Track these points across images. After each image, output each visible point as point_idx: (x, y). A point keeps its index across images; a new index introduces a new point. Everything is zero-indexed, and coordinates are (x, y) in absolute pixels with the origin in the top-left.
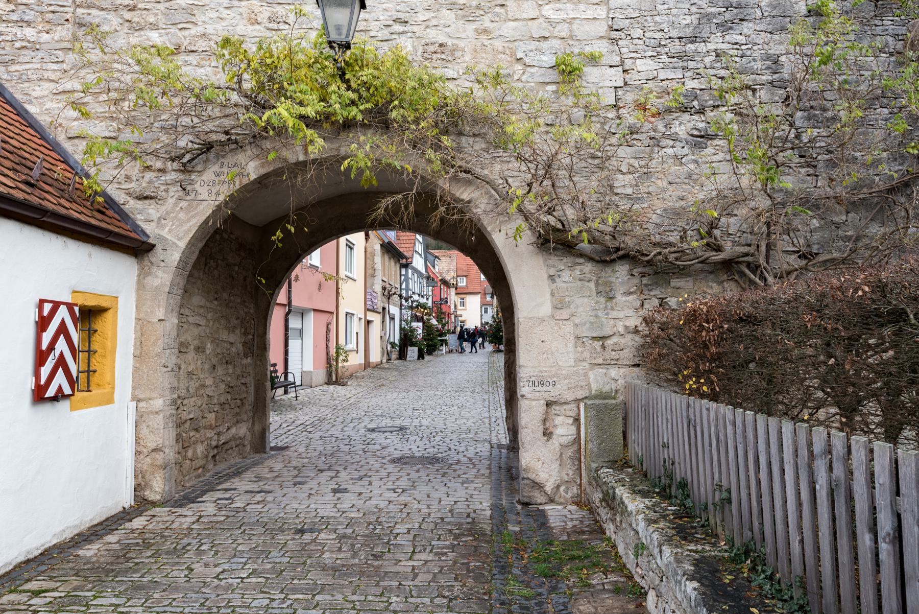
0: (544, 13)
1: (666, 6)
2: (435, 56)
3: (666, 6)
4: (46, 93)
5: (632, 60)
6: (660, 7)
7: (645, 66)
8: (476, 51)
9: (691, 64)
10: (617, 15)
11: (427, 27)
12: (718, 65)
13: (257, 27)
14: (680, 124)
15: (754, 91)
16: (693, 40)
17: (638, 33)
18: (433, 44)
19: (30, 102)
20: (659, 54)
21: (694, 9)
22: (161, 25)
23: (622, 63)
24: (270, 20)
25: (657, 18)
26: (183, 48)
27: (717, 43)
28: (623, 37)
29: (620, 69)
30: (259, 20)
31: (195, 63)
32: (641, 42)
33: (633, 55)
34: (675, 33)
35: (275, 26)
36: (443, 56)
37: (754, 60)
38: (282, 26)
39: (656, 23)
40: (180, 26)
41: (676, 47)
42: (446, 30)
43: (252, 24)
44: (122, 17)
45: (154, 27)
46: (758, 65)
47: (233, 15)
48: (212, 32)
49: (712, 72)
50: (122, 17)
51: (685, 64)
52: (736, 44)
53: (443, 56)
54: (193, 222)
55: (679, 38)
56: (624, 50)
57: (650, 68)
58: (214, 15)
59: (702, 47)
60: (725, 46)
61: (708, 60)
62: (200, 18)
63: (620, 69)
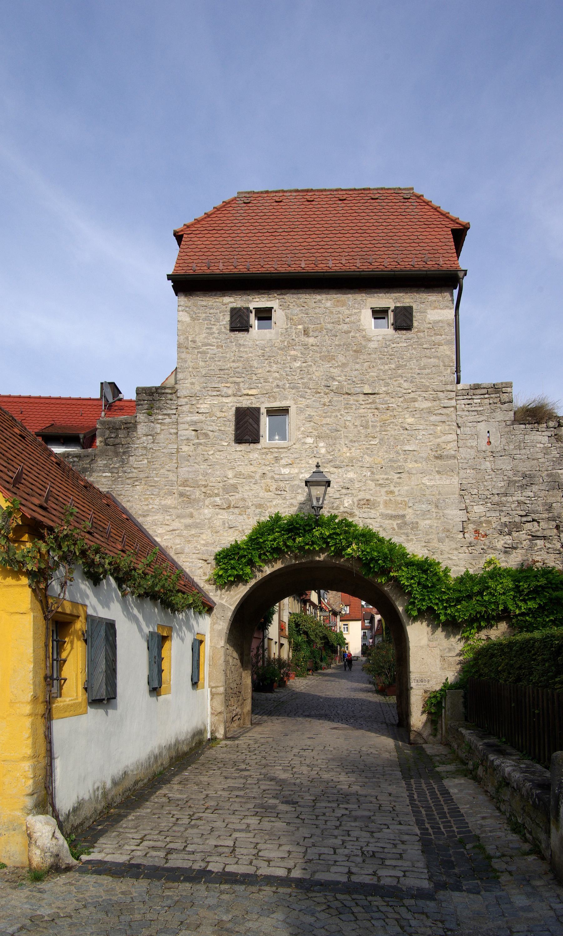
0: (423, 482)
1: (490, 477)
3: (490, 477)
4: (164, 531)
5: (471, 507)
7: (478, 509)
8: (386, 503)
9: (504, 508)
10: (464, 482)
11: (360, 491)
13: (270, 493)
14: (498, 541)
15: (538, 522)
16: (506, 495)
17: (475, 491)
19: (157, 536)
20: (486, 503)
21: (506, 478)
22: (220, 494)
23: (466, 508)
24: (277, 489)
25: (485, 483)
26: (232, 506)
27: (518, 496)
28: (467, 494)
29: (465, 511)
30: (271, 490)
31: (238, 513)
32: (477, 496)
33: (472, 504)
34: (495, 492)
35: (280, 493)
36: (369, 506)
37: (538, 506)
38: (283, 493)
39: (485, 486)
40: (231, 494)
41: (496, 499)
42: (371, 492)
43: (267, 492)
44: (201, 490)
45: (217, 495)
46: (540, 508)
47: (257, 487)
48: (247, 497)
49: (514, 512)
50: (201, 490)
51: (501, 508)
52: (529, 497)
53: (369, 506)
54: (239, 596)
55: (497, 494)
56: (467, 501)
57: (481, 511)
58: (247, 488)
59: (510, 499)
60: (523, 499)
61: (513, 506)
62: (240, 489)
63: (465, 511)
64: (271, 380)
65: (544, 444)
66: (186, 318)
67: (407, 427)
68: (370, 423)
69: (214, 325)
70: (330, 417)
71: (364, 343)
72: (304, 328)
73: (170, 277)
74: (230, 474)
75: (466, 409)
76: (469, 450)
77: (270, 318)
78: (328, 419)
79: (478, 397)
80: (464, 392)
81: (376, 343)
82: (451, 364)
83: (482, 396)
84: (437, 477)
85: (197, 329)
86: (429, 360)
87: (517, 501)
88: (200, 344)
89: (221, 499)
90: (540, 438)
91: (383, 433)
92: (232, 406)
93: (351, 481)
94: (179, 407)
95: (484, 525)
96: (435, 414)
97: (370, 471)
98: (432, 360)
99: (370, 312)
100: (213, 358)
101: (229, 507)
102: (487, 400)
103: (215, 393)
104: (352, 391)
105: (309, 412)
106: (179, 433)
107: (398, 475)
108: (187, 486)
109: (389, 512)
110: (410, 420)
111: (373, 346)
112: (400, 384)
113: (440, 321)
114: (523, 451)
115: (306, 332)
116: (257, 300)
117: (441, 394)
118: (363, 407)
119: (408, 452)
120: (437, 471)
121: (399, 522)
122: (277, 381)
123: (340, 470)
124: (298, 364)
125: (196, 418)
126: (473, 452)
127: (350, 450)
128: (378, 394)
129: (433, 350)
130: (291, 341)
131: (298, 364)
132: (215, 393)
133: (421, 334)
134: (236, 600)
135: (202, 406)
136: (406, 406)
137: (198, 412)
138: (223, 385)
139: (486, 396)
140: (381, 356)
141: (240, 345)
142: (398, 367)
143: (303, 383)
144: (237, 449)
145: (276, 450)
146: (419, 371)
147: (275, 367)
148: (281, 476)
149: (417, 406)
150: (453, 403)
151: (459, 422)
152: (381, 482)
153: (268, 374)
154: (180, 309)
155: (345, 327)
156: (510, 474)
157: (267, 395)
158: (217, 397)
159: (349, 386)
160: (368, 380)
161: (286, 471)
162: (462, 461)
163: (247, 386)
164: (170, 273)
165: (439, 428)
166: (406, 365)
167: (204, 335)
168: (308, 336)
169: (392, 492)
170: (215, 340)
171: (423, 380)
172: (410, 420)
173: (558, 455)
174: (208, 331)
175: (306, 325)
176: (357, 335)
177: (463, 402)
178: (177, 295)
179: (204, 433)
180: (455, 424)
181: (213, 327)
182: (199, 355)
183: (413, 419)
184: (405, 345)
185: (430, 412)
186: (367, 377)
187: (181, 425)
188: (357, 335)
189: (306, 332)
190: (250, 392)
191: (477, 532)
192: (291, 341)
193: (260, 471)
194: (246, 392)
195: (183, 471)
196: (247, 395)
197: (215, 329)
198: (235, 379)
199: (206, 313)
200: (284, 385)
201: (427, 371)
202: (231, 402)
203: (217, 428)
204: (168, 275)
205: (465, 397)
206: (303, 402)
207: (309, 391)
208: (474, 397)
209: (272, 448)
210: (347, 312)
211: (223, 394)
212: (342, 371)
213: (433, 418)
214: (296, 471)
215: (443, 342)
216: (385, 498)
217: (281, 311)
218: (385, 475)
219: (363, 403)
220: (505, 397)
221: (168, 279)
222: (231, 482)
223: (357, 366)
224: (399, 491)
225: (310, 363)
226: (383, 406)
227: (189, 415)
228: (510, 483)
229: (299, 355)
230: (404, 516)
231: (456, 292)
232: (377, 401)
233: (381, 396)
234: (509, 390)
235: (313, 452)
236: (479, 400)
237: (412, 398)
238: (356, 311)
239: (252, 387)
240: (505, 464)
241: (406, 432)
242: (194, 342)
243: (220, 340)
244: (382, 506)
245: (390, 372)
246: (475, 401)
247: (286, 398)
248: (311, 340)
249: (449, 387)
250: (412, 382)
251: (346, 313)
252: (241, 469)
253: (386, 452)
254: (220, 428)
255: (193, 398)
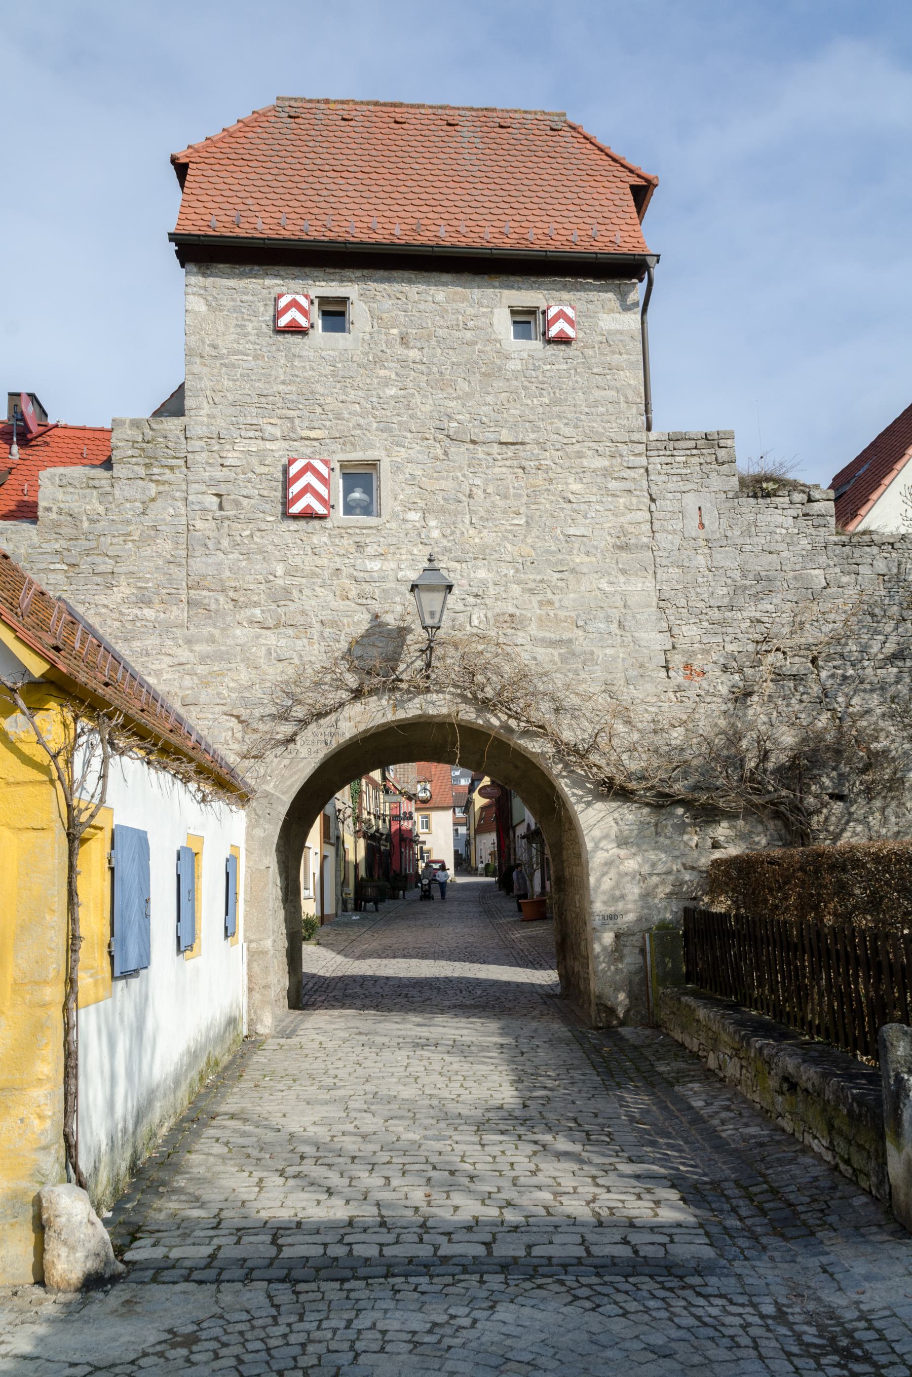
2: (505, 625)
6: (700, 580)
12: (751, 630)
18: (503, 614)
21: (729, 581)
25: (698, 589)
33: (678, 622)
63: (668, 634)
64: (346, 416)
65: (787, 529)
66: (198, 305)
67: (571, 497)
68: (512, 491)
69: (250, 320)
70: (446, 479)
71: (498, 362)
72: (401, 333)
73: (173, 237)
74: (280, 570)
75: (663, 472)
76: (670, 537)
77: (342, 314)
78: (443, 482)
79: (682, 452)
80: (659, 444)
81: (518, 362)
82: (638, 400)
83: (688, 452)
84: (622, 579)
85: (221, 328)
86: (603, 393)
87: (750, 618)
88: (225, 351)
89: (263, 612)
90: (780, 519)
91: (533, 507)
92: (281, 457)
93: (484, 583)
94: (190, 456)
95: (699, 656)
96: (615, 479)
97: (514, 567)
98: (608, 392)
99: (508, 311)
100: (248, 375)
101: (277, 626)
102: (697, 458)
103: (251, 434)
104: (481, 438)
105: (409, 469)
106: (190, 498)
107: (559, 575)
108: (205, 588)
109: (548, 635)
110: (576, 487)
111: (513, 367)
112: (558, 428)
113: (621, 332)
114: (756, 539)
115: (404, 340)
116: (323, 284)
117: (624, 446)
118: (500, 464)
119: (573, 538)
120: (620, 570)
121: (562, 651)
122: (358, 418)
123: (464, 565)
124: (392, 391)
125: (219, 474)
126: (677, 540)
127: (480, 532)
128: (522, 444)
129: (608, 377)
130: (379, 354)
131: (392, 391)
132: (251, 434)
133: (590, 352)
134: (292, 785)
135: (230, 455)
136: (567, 465)
137: (222, 465)
138: (265, 421)
139: (694, 452)
140: (526, 383)
141: (294, 356)
142: (555, 402)
143: (400, 423)
144: (291, 528)
145: (358, 531)
146: (587, 410)
147: (352, 395)
148: (366, 575)
149: (585, 464)
150: (643, 461)
151: (653, 492)
152: (532, 585)
153: (341, 405)
154: (189, 290)
155: (468, 335)
156: (737, 575)
157: (341, 441)
158: (254, 441)
159: (476, 430)
160: (506, 421)
161: (375, 565)
162: (661, 553)
163: (306, 424)
164: (172, 231)
165: (621, 500)
166: (566, 400)
167: (234, 336)
168: (408, 347)
169: (550, 603)
170: (251, 346)
171: (595, 425)
172: (576, 487)
173: (809, 547)
174: (239, 330)
175: (403, 329)
176: (488, 348)
177: (658, 460)
178: (183, 266)
179: (234, 500)
180: (646, 494)
181: (247, 323)
182: (224, 369)
183: (580, 486)
184: (565, 367)
185: (606, 473)
186: (505, 415)
187: (193, 486)
188: (488, 348)
189: (404, 340)
190: (313, 434)
191: (688, 666)
192: (379, 354)
193: (331, 565)
194: (306, 433)
195: (198, 565)
196: (308, 439)
197: (250, 327)
198: (285, 411)
199: (233, 300)
200: (369, 424)
201: (602, 409)
202: (278, 451)
203: (257, 492)
204: (170, 234)
205: (662, 453)
206: (402, 454)
207: (409, 435)
208: (675, 453)
209: (350, 528)
210: (471, 311)
211: (266, 435)
212: (464, 405)
213: (613, 485)
214: (393, 565)
215: (624, 365)
216: (538, 611)
217: (362, 303)
218: (538, 574)
219: (499, 457)
220: (722, 454)
221: (171, 240)
222: (280, 582)
223: (489, 399)
224: (560, 601)
225: (412, 391)
226: (532, 463)
227: (208, 469)
228: (737, 590)
229: (393, 376)
230: (570, 641)
231: (642, 287)
232: (522, 454)
233: (528, 447)
234: (729, 442)
235: (419, 535)
236: (684, 459)
237: (578, 452)
238: (484, 310)
239: (316, 424)
240: (727, 559)
241: (569, 506)
242: (215, 347)
243: (258, 347)
244: (533, 626)
245: (541, 410)
246: (678, 459)
247: (371, 446)
248: (413, 354)
249: (636, 437)
250: (576, 427)
251: (468, 313)
252: (298, 561)
253: (538, 537)
254: (262, 492)
255: (213, 441)
